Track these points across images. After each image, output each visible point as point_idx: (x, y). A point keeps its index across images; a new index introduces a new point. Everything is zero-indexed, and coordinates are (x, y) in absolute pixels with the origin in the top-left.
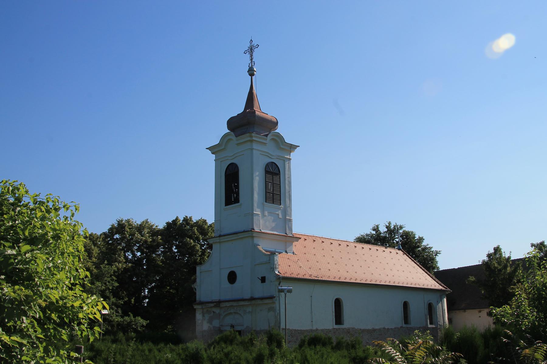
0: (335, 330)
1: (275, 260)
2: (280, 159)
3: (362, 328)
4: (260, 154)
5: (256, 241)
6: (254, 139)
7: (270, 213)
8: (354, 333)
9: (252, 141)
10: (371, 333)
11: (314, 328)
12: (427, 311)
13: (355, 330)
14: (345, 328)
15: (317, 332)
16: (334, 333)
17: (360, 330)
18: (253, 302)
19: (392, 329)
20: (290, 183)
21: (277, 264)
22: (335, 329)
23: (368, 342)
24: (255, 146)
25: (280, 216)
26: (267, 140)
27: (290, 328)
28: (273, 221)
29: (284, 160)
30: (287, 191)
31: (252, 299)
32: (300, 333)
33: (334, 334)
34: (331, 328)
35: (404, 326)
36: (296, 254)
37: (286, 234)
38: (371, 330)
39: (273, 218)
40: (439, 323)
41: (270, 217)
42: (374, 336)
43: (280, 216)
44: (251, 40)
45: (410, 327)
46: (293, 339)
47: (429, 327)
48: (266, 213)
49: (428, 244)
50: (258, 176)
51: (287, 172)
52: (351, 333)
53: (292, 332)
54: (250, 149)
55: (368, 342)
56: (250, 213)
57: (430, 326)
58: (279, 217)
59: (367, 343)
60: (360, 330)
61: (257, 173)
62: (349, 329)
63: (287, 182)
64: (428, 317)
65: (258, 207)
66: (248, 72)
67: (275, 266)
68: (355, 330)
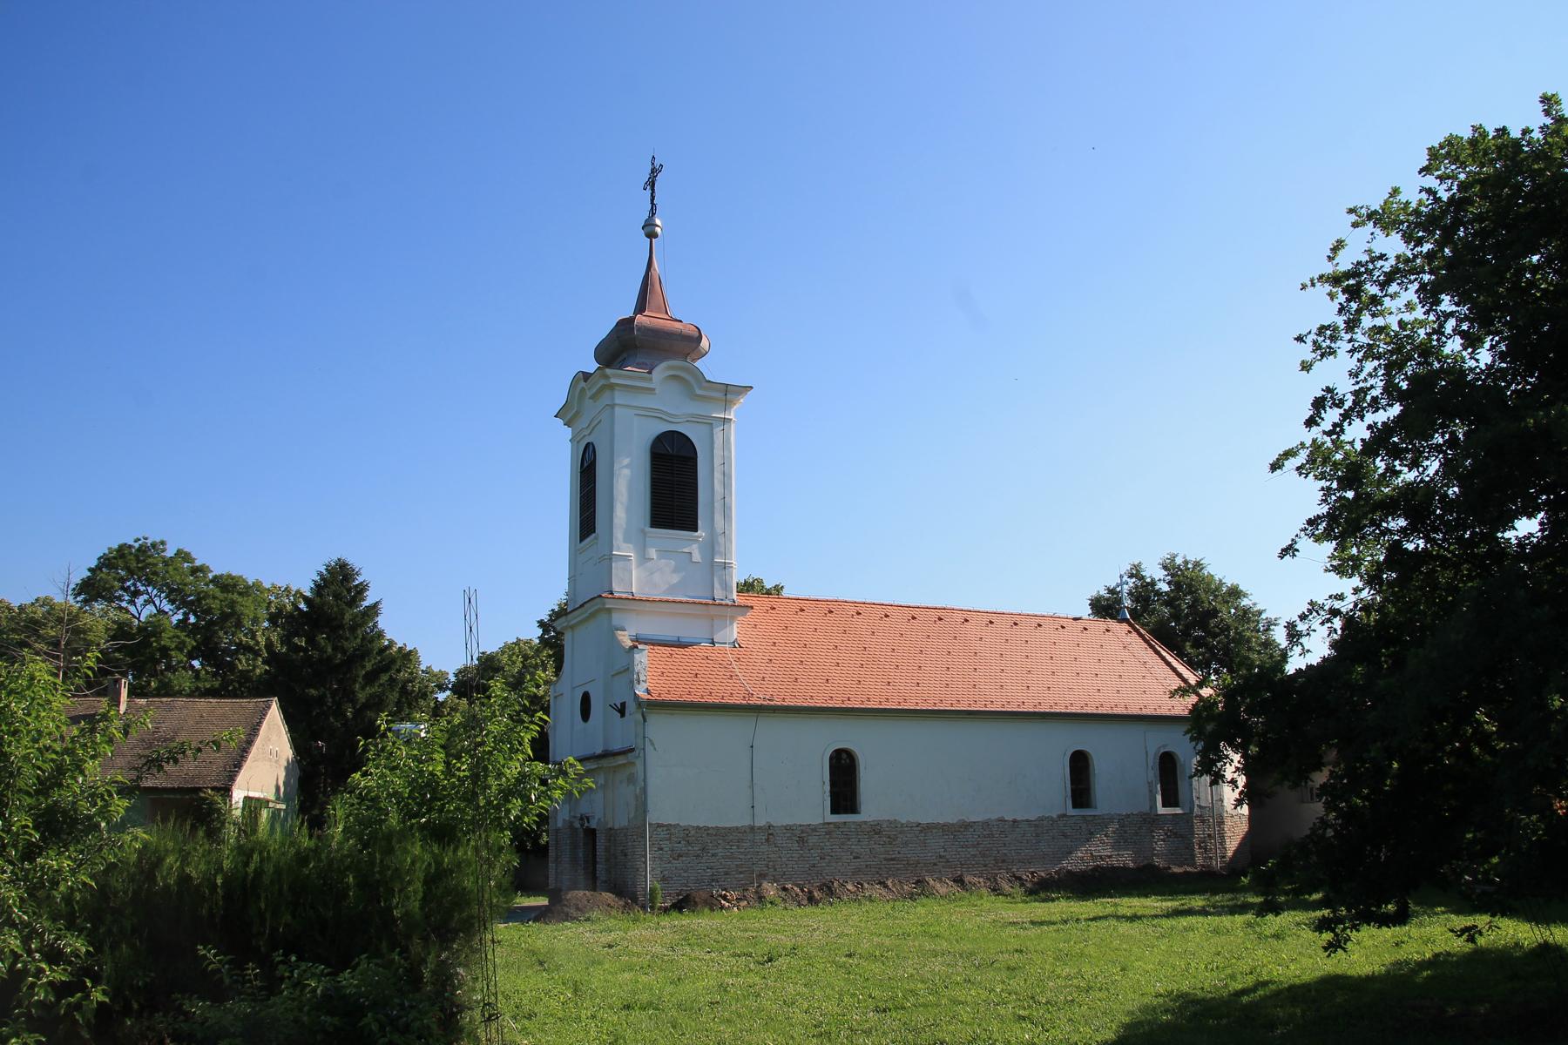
0: (832, 826)
1: (636, 663)
3: (924, 821)
5: (617, 619)
6: (613, 380)
7: (664, 553)
8: (894, 833)
9: (612, 387)
12: (1153, 774)
14: (865, 823)
15: (770, 832)
17: (917, 826)
18: (605, 763)
19: (1027, 821)
20: (726, 476)
21: (642, 671)
24: (619, 398)
25: (697, 557)
26: (651, 379)
27: (681, 824)
28: (675, 571)
30: (718, 497)
31: (606, 755)
32: (715, 835)
33: (828, 836)
35: (1071, 811)
36: (740, 647)
37: (714, 599)
38: (953, 825)
39: (673, 563)
40: (1197, 802)
41: (663, 561)
42: (964, 840)
43: (697, 557)
45: (1095, 816)
46: (690, 848)
47: (1159, 813)
48: (653, 553)
49: (1255, 604)
50: (627, 466)
51: (718, 452)
55: (942, 854)
56: (604, 555)
57: (1161, 810)
58: (644, 555)
59: (940, 857)
60: (917, 826)
61: (626, 461)
62: (879, 823)
63: (718, 475)
64: (1159, 789)
65: (627, 540)
66: (643, 228)
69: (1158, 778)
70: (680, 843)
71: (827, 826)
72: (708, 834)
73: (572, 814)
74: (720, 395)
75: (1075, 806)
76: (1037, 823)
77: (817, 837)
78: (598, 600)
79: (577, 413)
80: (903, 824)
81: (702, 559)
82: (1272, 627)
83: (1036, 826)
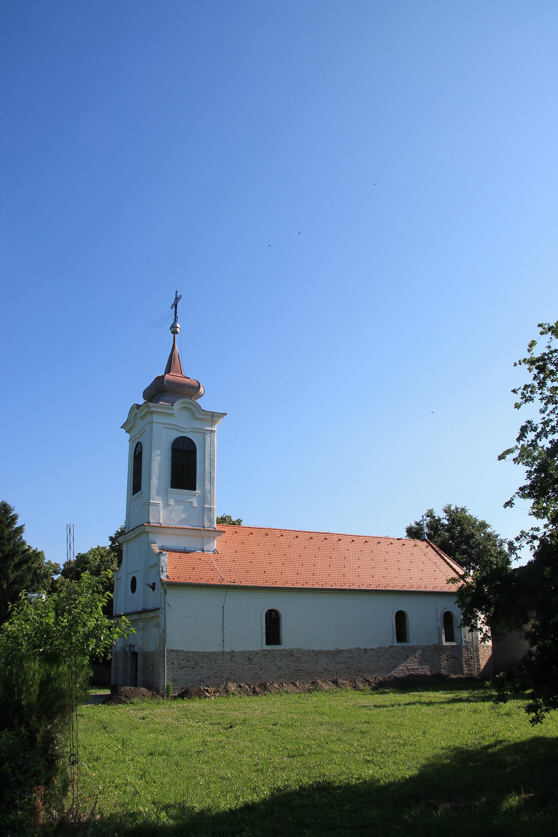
0: (266, 652)
1: (161, 561)
2: (197, 432)
3: (317, 649)
4: (164, 427)
5: (151, 537)
6: (152, 409)
7: (177, 502)
8: (300, 656)
9: (152, 413)
10: (333, 656)
11: (227, 649)
12: (440, 624)
13: (303, 652)
14: (284, 650)
15: (233, 655)
16: (264, 655)
17: (313, 652)
18: (143, 616)
19: (372, 649)
20: (212, 461)
21: (165, 566)
22: (265, 650)
23: (327, 668)
24: (156, 418)
25: (195, 504)
26: (173, 409)
27: (184, 650)
28: (184, 511)
29: (205, 433)
30: (207, 472)
31: (144, 611)
32: (203, 656)
33: (264, 657)
34: (258, 649)
35: (396, 644)
36: (218, 553)
37: (204, 527)
38: (332, 651)
39: (183, 507)
40: (464, 639)
42: (338, 660)
43: (195, 504)
44: (177, 291)
45: (409, 646)
46: (189, 663)
48: (172, 502)
49: (494, 531)
50: (159, 455)
51: (208, 448)
52: (295, 656)
53: (187, 654)
54: (149, 422)
56: (146, 503)
57: (445, 643)
58: (167, 503)
59: (325, 669)
60: (313, 652)
61: (158, 452)
62: (292, 650)
63: (207, 461)
64: (443, 631)
65: (158, 495)
67: (161, 568)
68: (303, 652)
69: (443, 626)
70: (183, 660)
71: (262, 652)
72: (199, 655)
73: (125, 643)
74: (210, 418)
75: (398, 641)
76: (378, 650)
77: (258, 658)
78: (142, 527)
79: (133, 426)
80: (304, 651)
81: (198, 505)
82: (503, 544)
83: (377, 652)
